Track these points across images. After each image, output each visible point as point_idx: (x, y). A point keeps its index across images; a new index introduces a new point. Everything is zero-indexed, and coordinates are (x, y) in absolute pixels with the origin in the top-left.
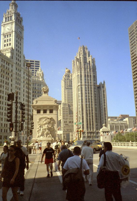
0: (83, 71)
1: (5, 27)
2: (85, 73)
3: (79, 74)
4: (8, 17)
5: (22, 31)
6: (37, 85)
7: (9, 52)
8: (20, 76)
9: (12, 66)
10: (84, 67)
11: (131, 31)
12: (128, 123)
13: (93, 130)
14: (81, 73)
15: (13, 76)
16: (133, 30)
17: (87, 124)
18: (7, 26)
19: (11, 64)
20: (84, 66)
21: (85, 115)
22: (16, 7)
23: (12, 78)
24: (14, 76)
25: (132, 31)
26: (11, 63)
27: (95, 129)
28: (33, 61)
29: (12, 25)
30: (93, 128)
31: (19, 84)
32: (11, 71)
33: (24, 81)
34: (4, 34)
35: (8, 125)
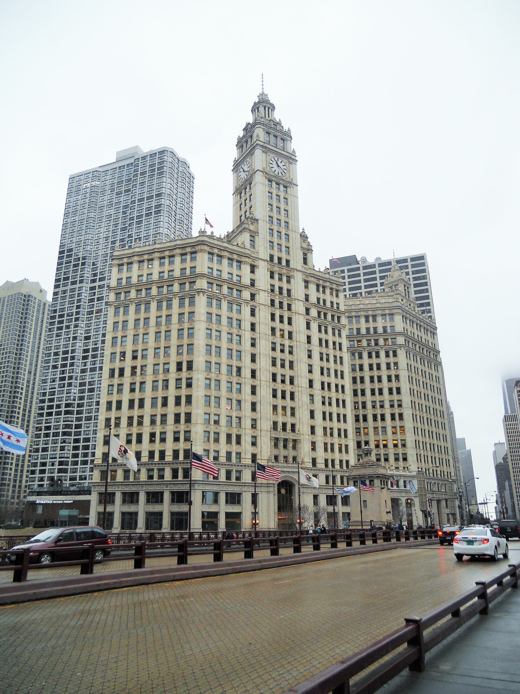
5: (291, 163)
6: (379, 319)
7: (241, 232)
8: (289, 295)
9: (252, 272)
15: (257, 297)
19: (245, 263)
22: (267, 108)
23: (252, 303)
24: (263, 298)
26: (247, 260)
28: (405, 260)
31: (286, 320)
32: (248, 283)
33: (307, 310)
35: (243, 456)
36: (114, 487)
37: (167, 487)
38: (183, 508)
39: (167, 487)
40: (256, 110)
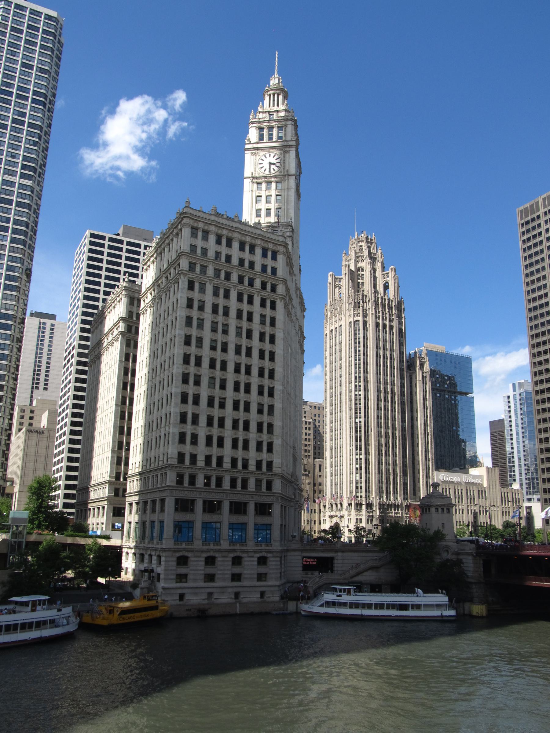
0: (371, 313)
1: (258, 157)
2: (377, 317)
3: (360, 318)
4: (271, 128)
10: (373, 299)
11: (529, 218)
12: (485, 485)
13: (396, 498)
14: (365, 316)
16: (535, 215)
17: (380, 481)
18: (267, 155)
20: (375, 297)
21: (375, 450)
25: (533, 220)
27: (401, 496)
29: (287, 155)
30: (395, 492)
34: (256, 178)
36: (195, 493)
37: (252, 497)
38: (265, 520)
39: (252, 497)
40: (276, 95)
